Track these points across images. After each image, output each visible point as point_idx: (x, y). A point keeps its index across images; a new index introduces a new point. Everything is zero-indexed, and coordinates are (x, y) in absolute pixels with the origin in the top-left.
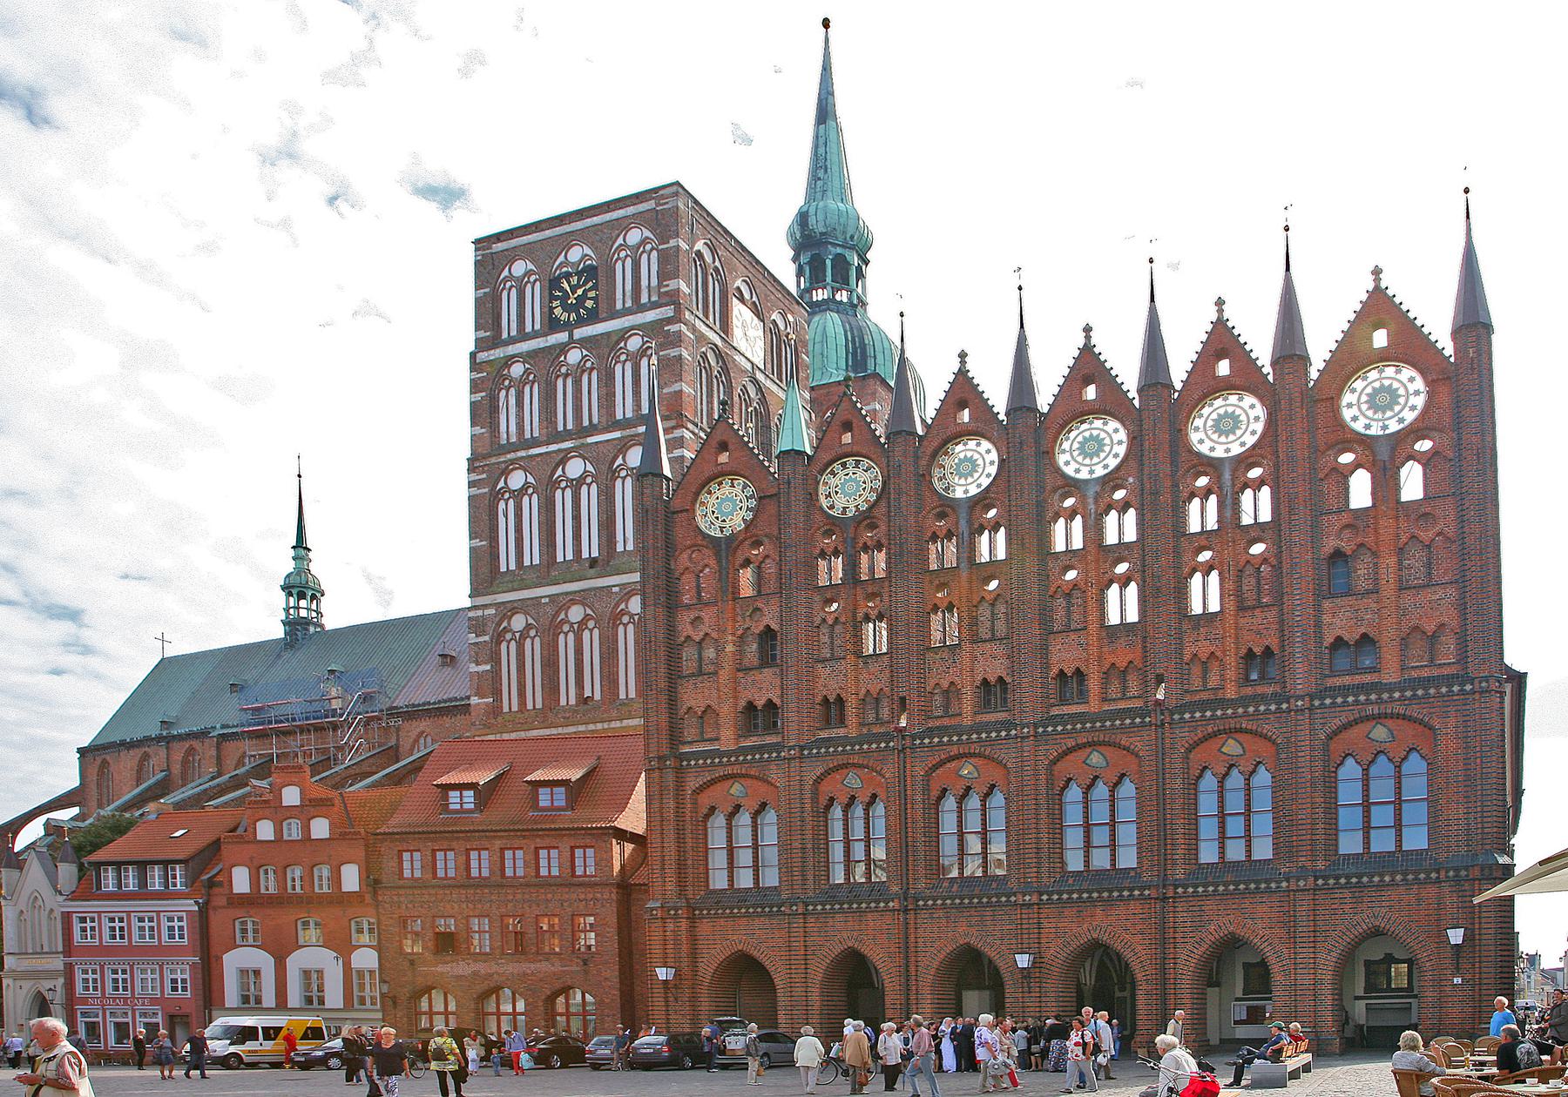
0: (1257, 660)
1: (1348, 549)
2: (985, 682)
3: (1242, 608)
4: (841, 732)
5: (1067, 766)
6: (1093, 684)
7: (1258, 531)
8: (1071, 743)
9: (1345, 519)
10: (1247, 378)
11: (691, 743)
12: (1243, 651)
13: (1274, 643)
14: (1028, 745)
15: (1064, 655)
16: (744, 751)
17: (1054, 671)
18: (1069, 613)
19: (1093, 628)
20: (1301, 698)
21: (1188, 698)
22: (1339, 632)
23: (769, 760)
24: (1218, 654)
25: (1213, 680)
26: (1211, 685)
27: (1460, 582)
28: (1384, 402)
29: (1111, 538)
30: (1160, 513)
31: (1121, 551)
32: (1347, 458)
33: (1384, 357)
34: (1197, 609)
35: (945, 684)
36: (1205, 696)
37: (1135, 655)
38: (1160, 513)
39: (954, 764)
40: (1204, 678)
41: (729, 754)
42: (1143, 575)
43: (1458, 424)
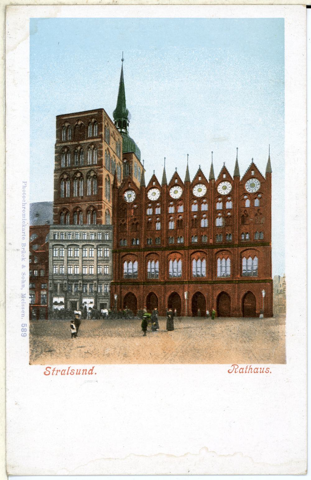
5: (195, 256)
7: (229, 210)
10: (229, 179)
28: (252, 186)
30: (212, 205)
31: (204, 212)
32: (245, 197)
33: (253, 177)
38: (212, 205)
42: (209, 218)
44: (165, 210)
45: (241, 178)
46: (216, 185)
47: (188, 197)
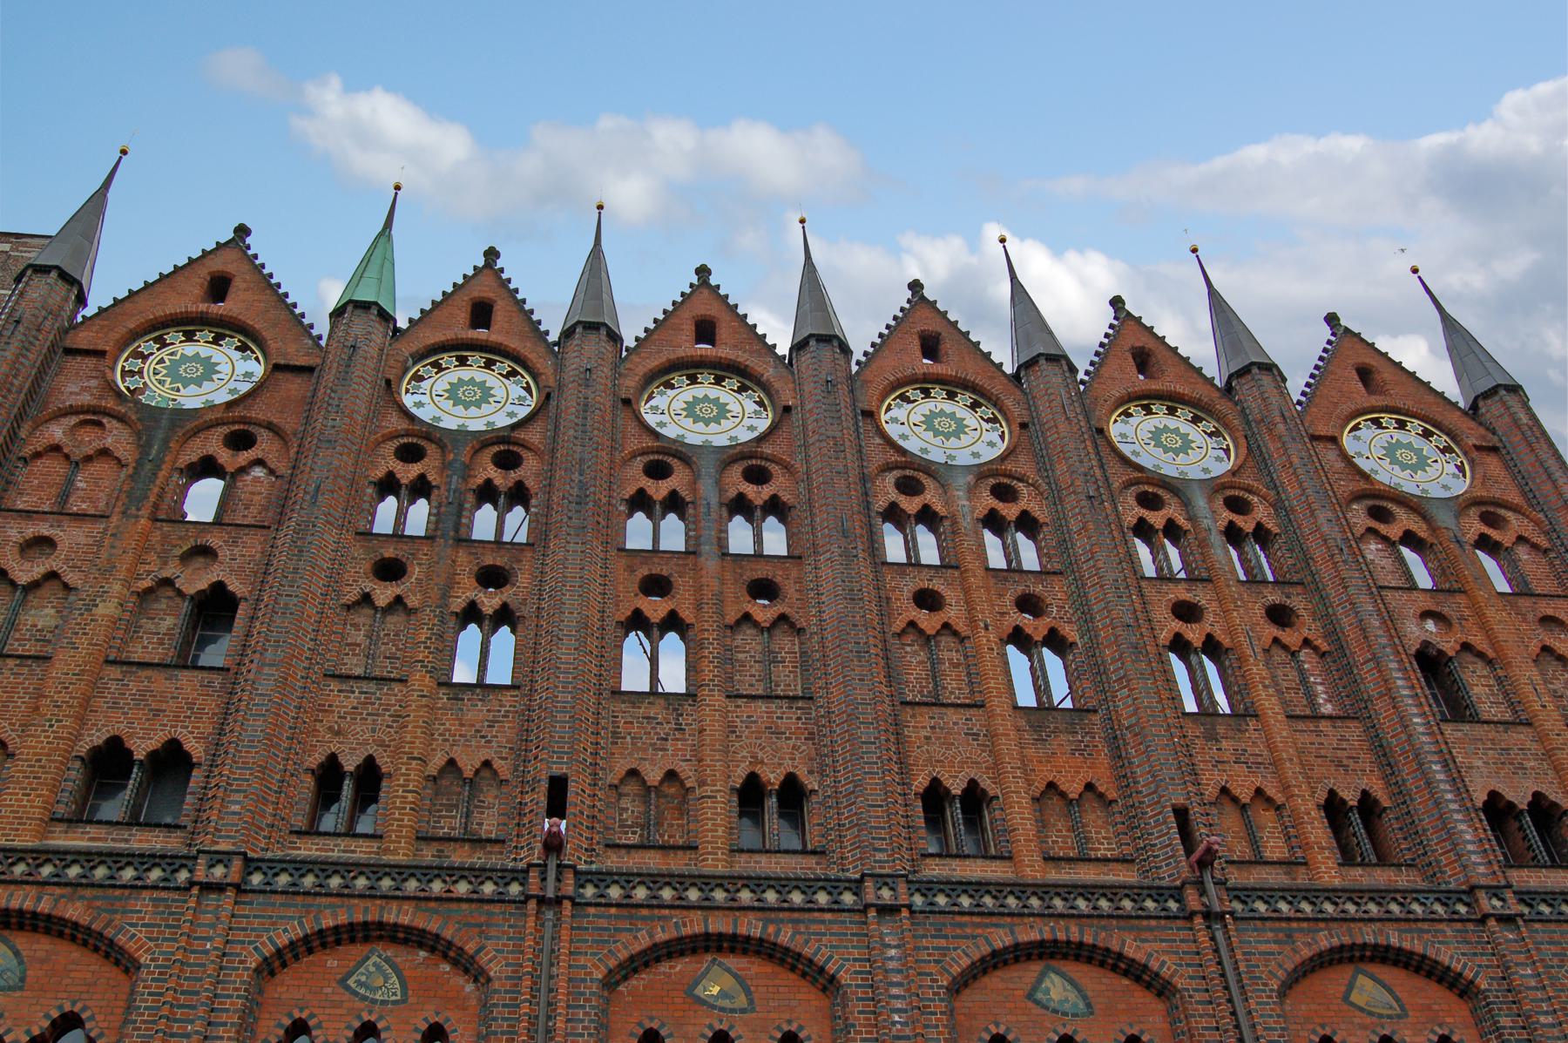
0: (1355, 822)
8: (1001, 938)
12: (1322, 796)
14: (887, 931)
17: (921, 782)
19: (998, 705)
24: (1271, 791)
35: (654, 775)
39: (680, 966)
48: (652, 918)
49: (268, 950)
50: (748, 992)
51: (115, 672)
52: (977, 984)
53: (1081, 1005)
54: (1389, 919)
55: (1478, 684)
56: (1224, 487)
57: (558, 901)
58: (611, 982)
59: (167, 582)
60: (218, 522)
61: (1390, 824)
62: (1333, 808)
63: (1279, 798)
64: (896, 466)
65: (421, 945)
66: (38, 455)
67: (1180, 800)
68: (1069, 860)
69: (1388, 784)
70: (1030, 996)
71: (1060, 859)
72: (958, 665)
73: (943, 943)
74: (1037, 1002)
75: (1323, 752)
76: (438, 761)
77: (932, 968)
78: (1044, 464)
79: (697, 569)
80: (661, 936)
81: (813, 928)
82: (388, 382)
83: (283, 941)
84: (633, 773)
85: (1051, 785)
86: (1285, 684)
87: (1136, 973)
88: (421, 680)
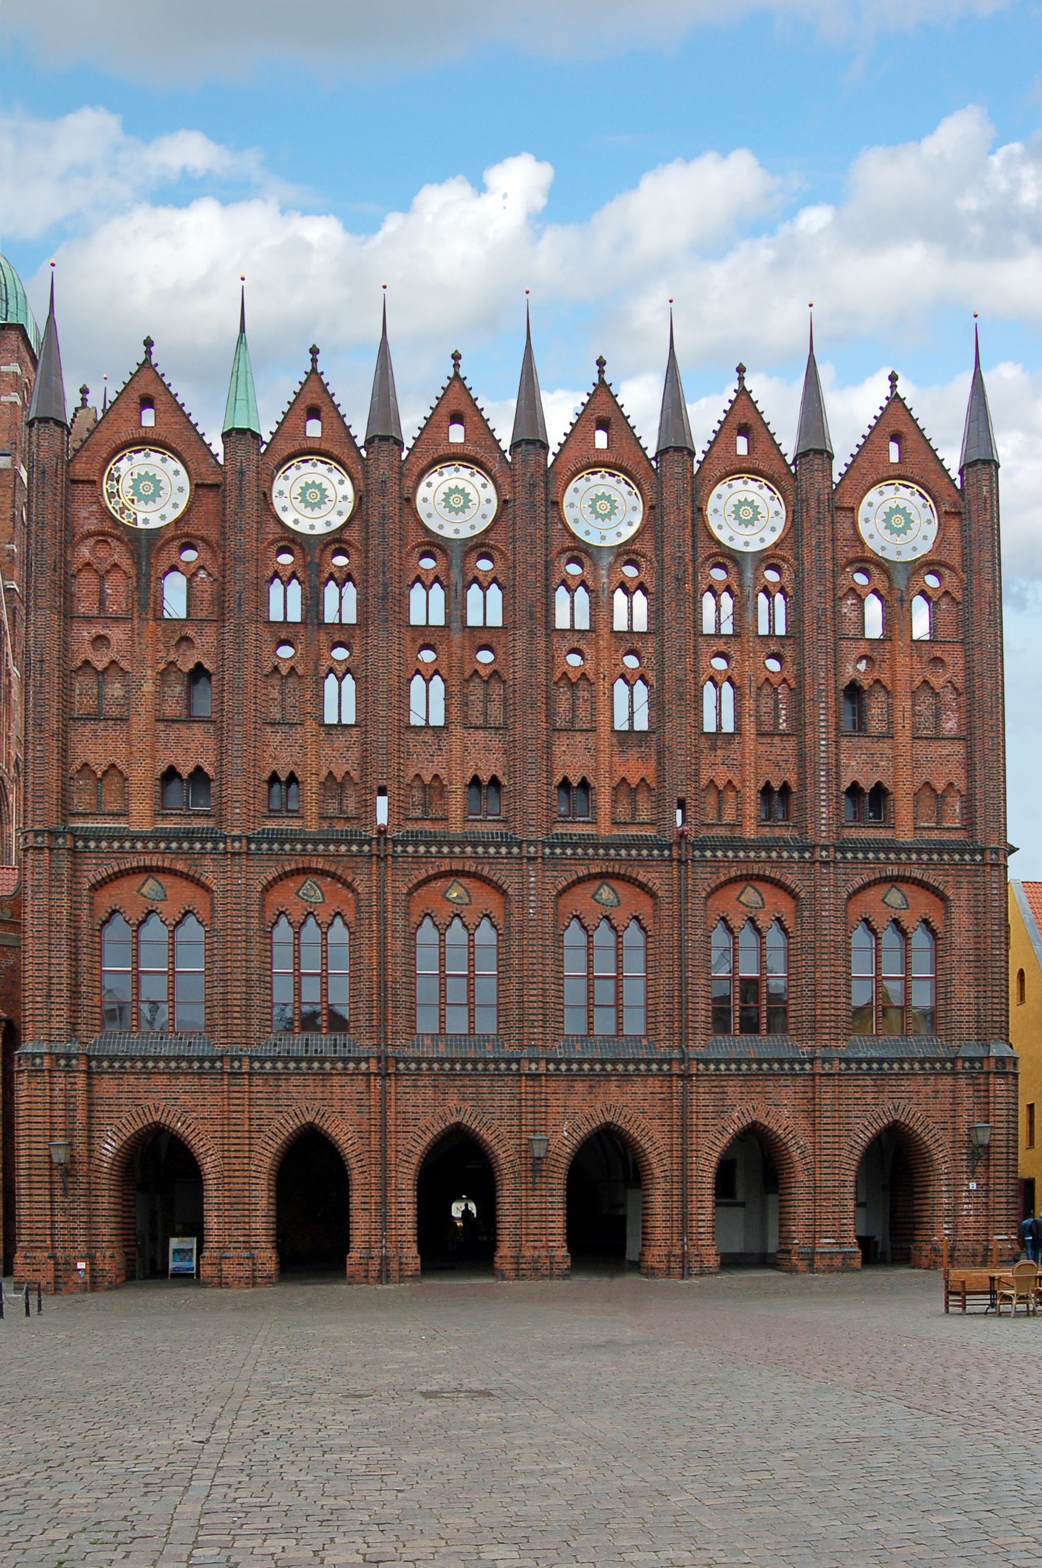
0: (776, 798)
1: (865, 684)
2: (475, 781)
3: (760, 734)
4: (295, 824)
5: (579, 900)
6: (603, 798)
8: (582, 871)
9: (863, 648)
11: (85, 815)
12: (762, 784)
13: (792, 779)
15: (572, 760)
16: (167, 836)
17: (558, 779)
18: (573, 709)
19: (604, 731)
20: (825, 847)
21: (704, 833)
22: (857, 778)
23: (203, 853)
25: (729, 815)
26: (727, 819)
27: (967, 737)
29: (620, 623)
30: (674, 604)
32: (860, 579)
34: (709, 725)
35: (428, 778)
36: (723, 832)
37: (649, 771)
38: (674, 604)
39: (439, 883)
40: (720, 810)
41: (144, 838)
43: (967, 564)
44: (383, 604)
45: (838, 467)
46: (697, 490)
47: (529, 538)
48: (426, 863)
49: (265, 882)
50: (469, 896)
51: (161, 726)
52: (570, 891)
53: (615, 901)
54: (769, 860)
55: (876, 709)
56: (768, 557)
57: (386, 856)
58: (410, 893)
59: (172, 663)
60: (189, 619)
61: (793, 799)
62: (766, 791)
63: (738, 786)
64: (569, 549)
65: (328, 876)
66: (80, 571)
67: (682, 795)
68: (625, 823)
69: (799, 779)
70: (593, 897)
71: (620, 823)
72: (586, 701)
73: (555, 874)
74: (596, 900)
75: (770, 758)
76: (324, 773)
77: (549, 886)
78: (659, 547)
79: (449, 640)
80: (431, 872)
81: (499, 867)
82: (265, 494)
83: (270, 878)
84: (418, 775)
85: (624, 779)
86: (764, 710)
87: (642, 886)
88: (311, 724)
